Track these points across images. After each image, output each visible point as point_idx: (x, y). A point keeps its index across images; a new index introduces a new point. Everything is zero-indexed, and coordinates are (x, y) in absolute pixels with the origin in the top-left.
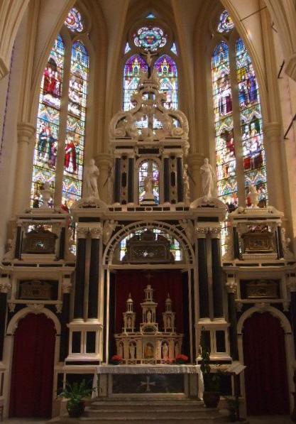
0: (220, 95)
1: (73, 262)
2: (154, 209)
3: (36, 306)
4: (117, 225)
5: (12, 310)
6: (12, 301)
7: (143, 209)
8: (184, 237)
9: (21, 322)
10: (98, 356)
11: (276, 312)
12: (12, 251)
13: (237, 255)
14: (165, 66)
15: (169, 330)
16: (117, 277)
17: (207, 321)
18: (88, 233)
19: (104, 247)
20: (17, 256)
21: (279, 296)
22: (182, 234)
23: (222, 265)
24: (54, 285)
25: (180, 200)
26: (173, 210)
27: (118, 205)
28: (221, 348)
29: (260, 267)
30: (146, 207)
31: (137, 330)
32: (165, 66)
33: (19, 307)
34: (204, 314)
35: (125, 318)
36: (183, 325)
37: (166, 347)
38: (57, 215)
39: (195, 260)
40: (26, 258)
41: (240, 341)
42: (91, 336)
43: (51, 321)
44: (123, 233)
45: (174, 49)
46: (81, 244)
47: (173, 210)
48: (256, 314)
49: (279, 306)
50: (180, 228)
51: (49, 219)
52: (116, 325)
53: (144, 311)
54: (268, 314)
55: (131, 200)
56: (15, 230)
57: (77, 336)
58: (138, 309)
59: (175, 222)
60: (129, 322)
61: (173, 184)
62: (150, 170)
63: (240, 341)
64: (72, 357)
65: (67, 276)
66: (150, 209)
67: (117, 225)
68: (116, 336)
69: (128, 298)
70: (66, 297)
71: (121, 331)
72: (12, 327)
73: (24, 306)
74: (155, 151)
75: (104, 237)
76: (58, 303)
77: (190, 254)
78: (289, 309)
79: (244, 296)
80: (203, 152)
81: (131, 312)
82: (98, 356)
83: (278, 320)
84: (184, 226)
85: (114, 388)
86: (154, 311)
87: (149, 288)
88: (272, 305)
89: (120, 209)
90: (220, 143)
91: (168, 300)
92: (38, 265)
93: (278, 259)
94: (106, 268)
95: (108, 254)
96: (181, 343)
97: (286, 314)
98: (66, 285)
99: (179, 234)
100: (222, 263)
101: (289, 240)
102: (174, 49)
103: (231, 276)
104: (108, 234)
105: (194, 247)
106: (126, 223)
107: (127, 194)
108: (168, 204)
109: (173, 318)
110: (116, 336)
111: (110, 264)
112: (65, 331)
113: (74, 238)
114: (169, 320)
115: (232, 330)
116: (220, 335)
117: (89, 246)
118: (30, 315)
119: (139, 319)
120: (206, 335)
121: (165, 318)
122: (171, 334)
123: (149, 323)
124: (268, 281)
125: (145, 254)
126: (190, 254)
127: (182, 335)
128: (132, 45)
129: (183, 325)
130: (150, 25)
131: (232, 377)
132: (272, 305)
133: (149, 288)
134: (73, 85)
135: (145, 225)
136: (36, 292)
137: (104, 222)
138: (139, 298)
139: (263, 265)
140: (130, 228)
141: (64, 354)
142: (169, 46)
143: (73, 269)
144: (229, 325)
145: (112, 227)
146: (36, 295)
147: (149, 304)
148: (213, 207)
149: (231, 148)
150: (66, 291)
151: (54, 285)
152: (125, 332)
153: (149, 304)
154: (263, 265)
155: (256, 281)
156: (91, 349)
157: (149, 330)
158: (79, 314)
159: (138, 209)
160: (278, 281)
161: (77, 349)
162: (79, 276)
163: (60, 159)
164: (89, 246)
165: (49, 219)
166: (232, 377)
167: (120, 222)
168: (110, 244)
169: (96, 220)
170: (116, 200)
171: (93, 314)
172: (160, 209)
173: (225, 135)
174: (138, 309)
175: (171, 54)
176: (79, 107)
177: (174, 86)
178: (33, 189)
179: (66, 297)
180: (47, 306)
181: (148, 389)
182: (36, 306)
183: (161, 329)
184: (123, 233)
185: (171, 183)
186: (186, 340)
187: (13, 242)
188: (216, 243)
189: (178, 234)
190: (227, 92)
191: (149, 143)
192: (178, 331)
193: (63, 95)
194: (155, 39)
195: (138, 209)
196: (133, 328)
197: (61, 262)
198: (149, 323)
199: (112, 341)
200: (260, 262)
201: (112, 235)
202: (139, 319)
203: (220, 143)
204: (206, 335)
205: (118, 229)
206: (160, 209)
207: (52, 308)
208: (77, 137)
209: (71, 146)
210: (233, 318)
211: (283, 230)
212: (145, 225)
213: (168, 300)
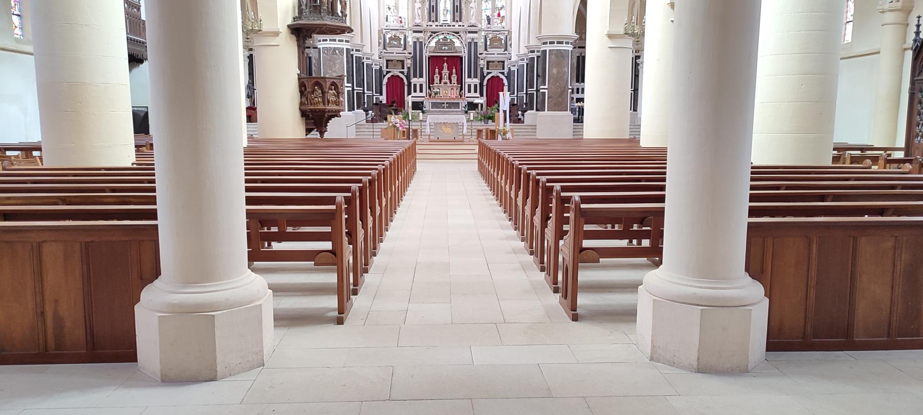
1: (410, 52)
2: (448, 26)
3: (396, 72)
4: (430, 34)
5: (385, 74)
6: (384, 69)
7: (442, 26)
8: (462, 40)
9: (389, 78)
10: (424, 94)
11: (501, 76)
12: (382, 45)
13: (486, 49)
15: (454, 83)
16: (430, 58)
17: (469, 80)
18: (418, 39)
19: (425, 44)
21: (504, 69)
22: (461, 39)
23: (478, 54)
24: (403, 62)
25: (460, 21)
26: (457, 26)
27: (430, 23)
29: (496, 55)
30: (444, 25)
31: (440, 83)
33: (388, 72)
34: (469, 77)
35: (435, 78)
36: (460, 81)
37: (452, 90)
38: (402, 28)
39: (466, 52)
40: (389, 49)
41: (485, 88)
42: (421, 86)
43: (402, 79)
44: (433, 38)
46: (415, 43)
47: (457, 26)
48: (493, 77)
49: (503, 73)
50: (460, 36)
51: (398, 30)
52: (431, 81)
53: (443, 75)
54: (498, 76)
55: (437, 21)
56: (382, 35)
57: (415, 85)
58: (440, 74)
59: (457, 33)
60: (437, 79)
61: (457, 12)
63: (485, 88)
64: (413, 94)
65: (409, 59)
66: (445, 26)
67: (430, 34)
68: (431, 85)
69: (436, 68)
70: (409, 68)
71: (433, 84)
72: (385, 81)
73: (390, 72)
75: (425, 39)
76: (405, 70)
77: (464, 48)
78: (508, 74)
79: (488, 69)
81: (437, 75)
82: (424, 94)
83: (502, 80)
84: (462, 35)
85: (432, 107)
86: (448, 75)
87: (445, 64)
88: (500, 73)
89: (431, 26)
91: (454, 70)
92: (395, 53)
93: (504, 51)
94: (426, 54)
95: (427, 48)
96: (459, 89)
97: (506, 77)
98: (408, 63)
100: (478, 53)
101: (510, 42)
103: (482, 59)
104: (427, 38)
105: (466, 45)
106: (435, 33)
107: (435, 16)
108: (454, 23)
109: (456, 78)
110: (431, 85)
111: (428, 52)
112: (409, 84)
113: (410, 41)
114: (454, 78)
115: (481, 84)
116: (476, 86)
120: (469, 86)
121: (452, 78)
122: (455, 85)
123: (445, 80)
124: (499, 62)
125: (443, 48)
126: (464, 48)
127: (460, 85)
131: (480, 105)
132: (500, 73)
133: (445, 64)
135: (443, 34)
136: (395, 65)
137: (425, 32)
138: (441, 69)
139: (498, 54)
140: (437, 35)
141: (409, 93)
143: (412, 55)
144: (480, 82)
145: (429, 34)
146: (395, 67)
147: (445, 71)
148: (475, 26)
150: (409, 66)
151: (403, 62)
152: (435, 84)
153: (445, 71)
154: (498, 54)
155: (493, 62)
156: (421, 91)
157: (445, 83)
158: (415, 76)
159: (440, 26)
160: (503, 62)
162: (414, 58)
164: (419, 46)
165: (398, 30)
166: (480, 105)
167: (432, 32)
168: (427, 43)
169: (421, 32)
170: (430, 21)
171: (421, 76)
172: (450, 26)
174: (440, 74)
178: (386, 10)
180: (400, 72)
181: (445, 107)
182: (396, 72)
183: (451, 83)
184: (433, 38)
188: (476, 44)
189: (459, 39)
192: (458, 84)
195: (440, 26)
196: (438, 82)
197: (405, 51)
198: (445, 80)
200: (495, 54)
201: (429, 38)
205: (431, 36)
206: (450, 26)
207: (403, 73)
210: (483, 77)
211: (508, 37)
212: (443, 34)
213: (454, 70)
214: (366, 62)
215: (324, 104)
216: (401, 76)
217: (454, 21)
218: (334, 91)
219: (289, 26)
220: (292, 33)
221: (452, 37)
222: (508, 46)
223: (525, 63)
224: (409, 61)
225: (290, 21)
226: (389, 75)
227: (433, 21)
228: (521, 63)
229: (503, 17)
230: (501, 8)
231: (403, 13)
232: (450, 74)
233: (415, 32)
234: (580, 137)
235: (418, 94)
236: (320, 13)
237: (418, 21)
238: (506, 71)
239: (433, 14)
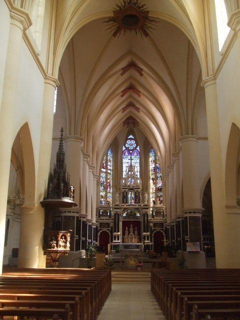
0: (152, 166)
6: (99, 228)
11: (162, 231)
14: (135, 154)
17: (145, 233)
18: (117, 212)
20: (99, 217)
28: (148, 240)
32: (135, 154)
33: (100, 230)
34: (144, 232)
36: (139, 234)
40: (102, 218)
42: (118, 237)
45: (138, 148)
46: (115, 214)
48: (157, 232)
49: (163, 230)
52: (124, 234)
57: (115, 236)
58: (129, 230)
59: (138, 209)
60: (127, 233)
62: (131, 194)
63: (153, 238)
70: (112, 227)
72: (99, 234)
73: (101, 229)
74: (132, 189)
76: (110, 229)
80: (146, 188)
90: (151, 181)
92: (105, 220)
94: (121, 220)
98: (112, 225)
99: (139, 212)
102: (138, 148)
112: (112, 235)
114: (136, 232)
115: (151, 235)
116: (148, 236)
117: (117, 215)
118: (103, 231)
119: (129, 232)
128: (125, 147)
129: (139, 234)
130: (131, 139)
134: (109, 164)
141: (112, 241)
142: (137, 147)
145: (122, 210)
147: (131, 229)
149: (154, 183)
151: (108, 224)
153: (131, 229)
156: (118, 240)
160: (163, 224)
161: (115, 240)
162: (115, 222)
163: (105, 189)
164: (117, 215)
171: (118, 232)
173: (153, 179)
175: (137, 150)
176: (110, 170)
177: (138, 161)
179: (112, 227)
182: (105, 229)
185: (137, 199)
186: (140, 237)
187: (98, 214)
190: (154, 166)
191: (131, 187)
193: (106, 168)
194: (132, 145)
199: (123, 238)
200: (158, 219)
202: (129, 232)
203: (151, 181)
204: (145, 236)
207: (108, 230)
208: (110, 181)
209: (109, 183)
210: (151, 232)
214: (89, 224)
215: (57, 247)
216: (108, 231)
217: (135, 202)
218: (64, 240)
219: (41, 203)
220: (43, 206)
221: (135, 211)
222: (165, 216)
223: (174, 224)
224: (112, 224)
225: (42, 200)
226: (101, 231)
227: (125, 203)
228: (172, 224)
229: (162, 201)
230: (160, 197)
231: (110, 199)
232: (134, 231)
233: (115, 209)
234: (214, 268)
235: (117, 241)
236: (60, 196)
237: (117, 203)
238: (164, 228)
239: (125, 200)
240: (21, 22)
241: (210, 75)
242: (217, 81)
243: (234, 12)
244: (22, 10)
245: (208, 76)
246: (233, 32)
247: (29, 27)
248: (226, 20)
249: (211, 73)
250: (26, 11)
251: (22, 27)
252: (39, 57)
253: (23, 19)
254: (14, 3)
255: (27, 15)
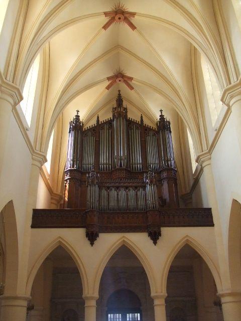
240: (12, 96)
241: (204, 150)
242: (213, 155)
243: (226, 87)
244: (14, 85)
245: (202, 151)
246: (226, 108)
247: (19, 102)
248: (219, 94)
249: (205, 148)
250: (17, 87)
251: (12, 102)
252: (27, 132)
253: (13, 93)
254: (6, 79)
255: (18, 90)
